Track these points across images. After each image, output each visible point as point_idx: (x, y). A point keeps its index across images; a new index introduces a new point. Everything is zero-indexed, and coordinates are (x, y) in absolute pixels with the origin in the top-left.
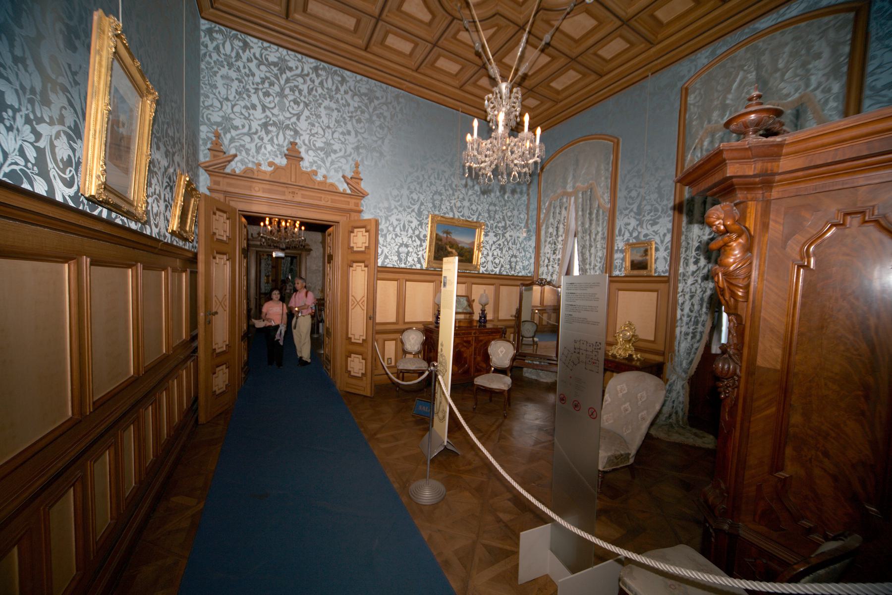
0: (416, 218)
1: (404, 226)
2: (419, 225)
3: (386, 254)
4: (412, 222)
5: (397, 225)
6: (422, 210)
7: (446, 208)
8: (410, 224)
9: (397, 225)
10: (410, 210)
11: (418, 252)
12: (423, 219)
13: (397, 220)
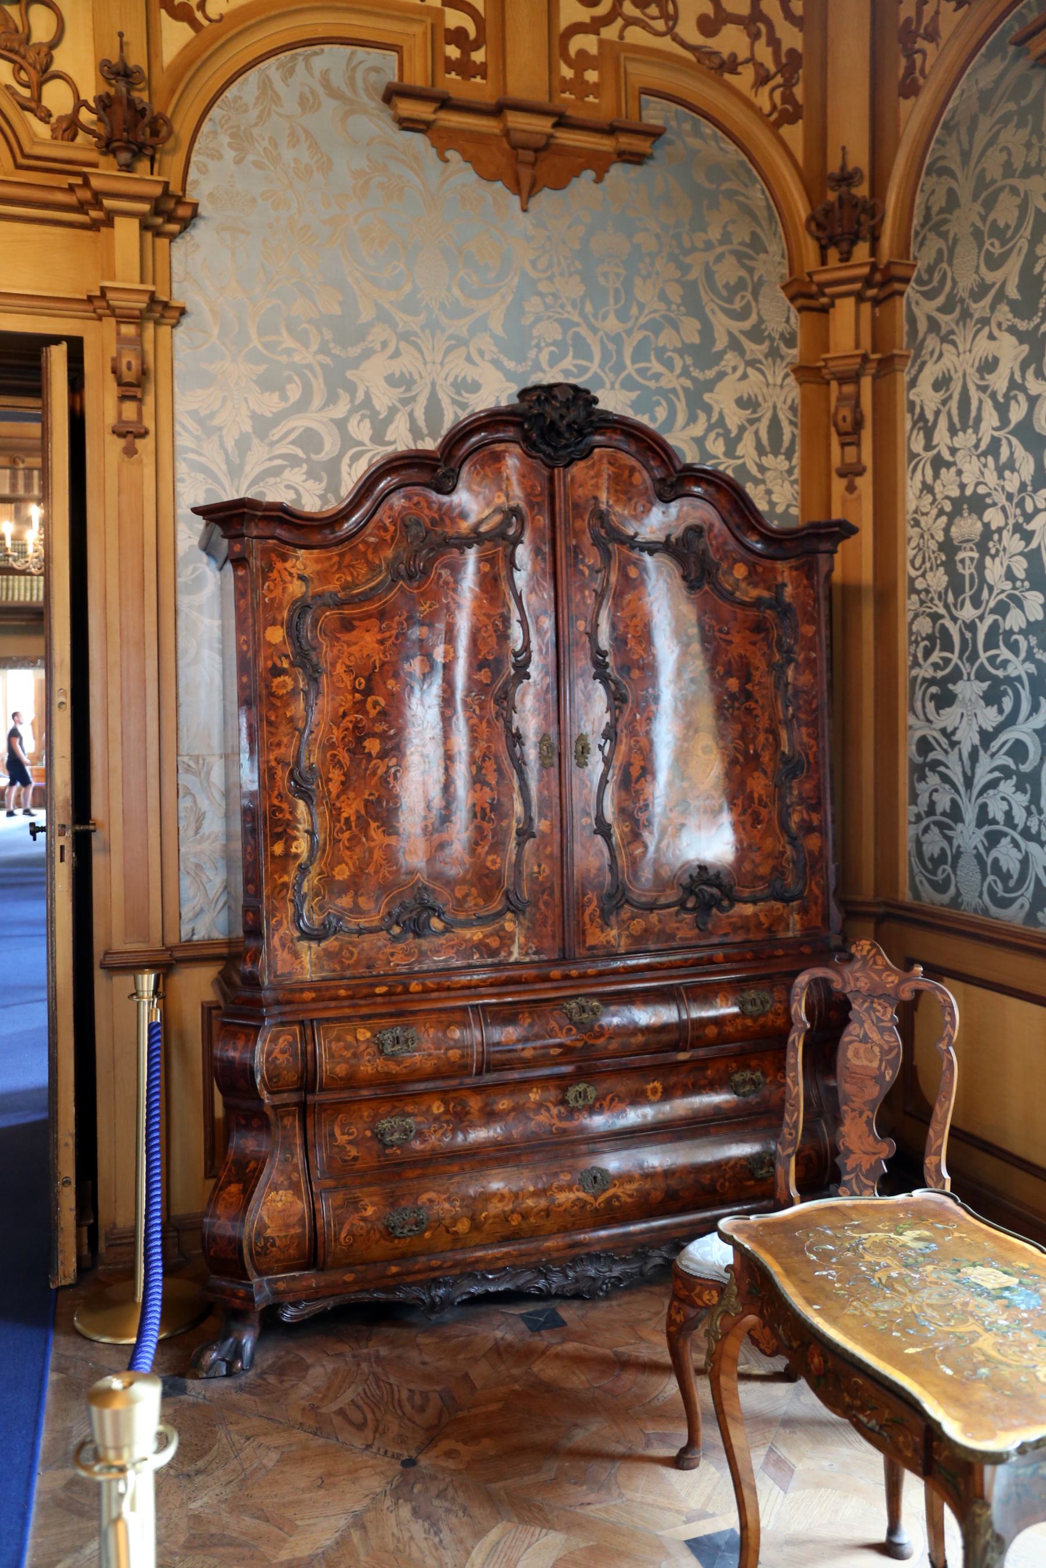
0: (496, 363)
9: (393, 411)
10: (461, 328)
13: (392, 381)
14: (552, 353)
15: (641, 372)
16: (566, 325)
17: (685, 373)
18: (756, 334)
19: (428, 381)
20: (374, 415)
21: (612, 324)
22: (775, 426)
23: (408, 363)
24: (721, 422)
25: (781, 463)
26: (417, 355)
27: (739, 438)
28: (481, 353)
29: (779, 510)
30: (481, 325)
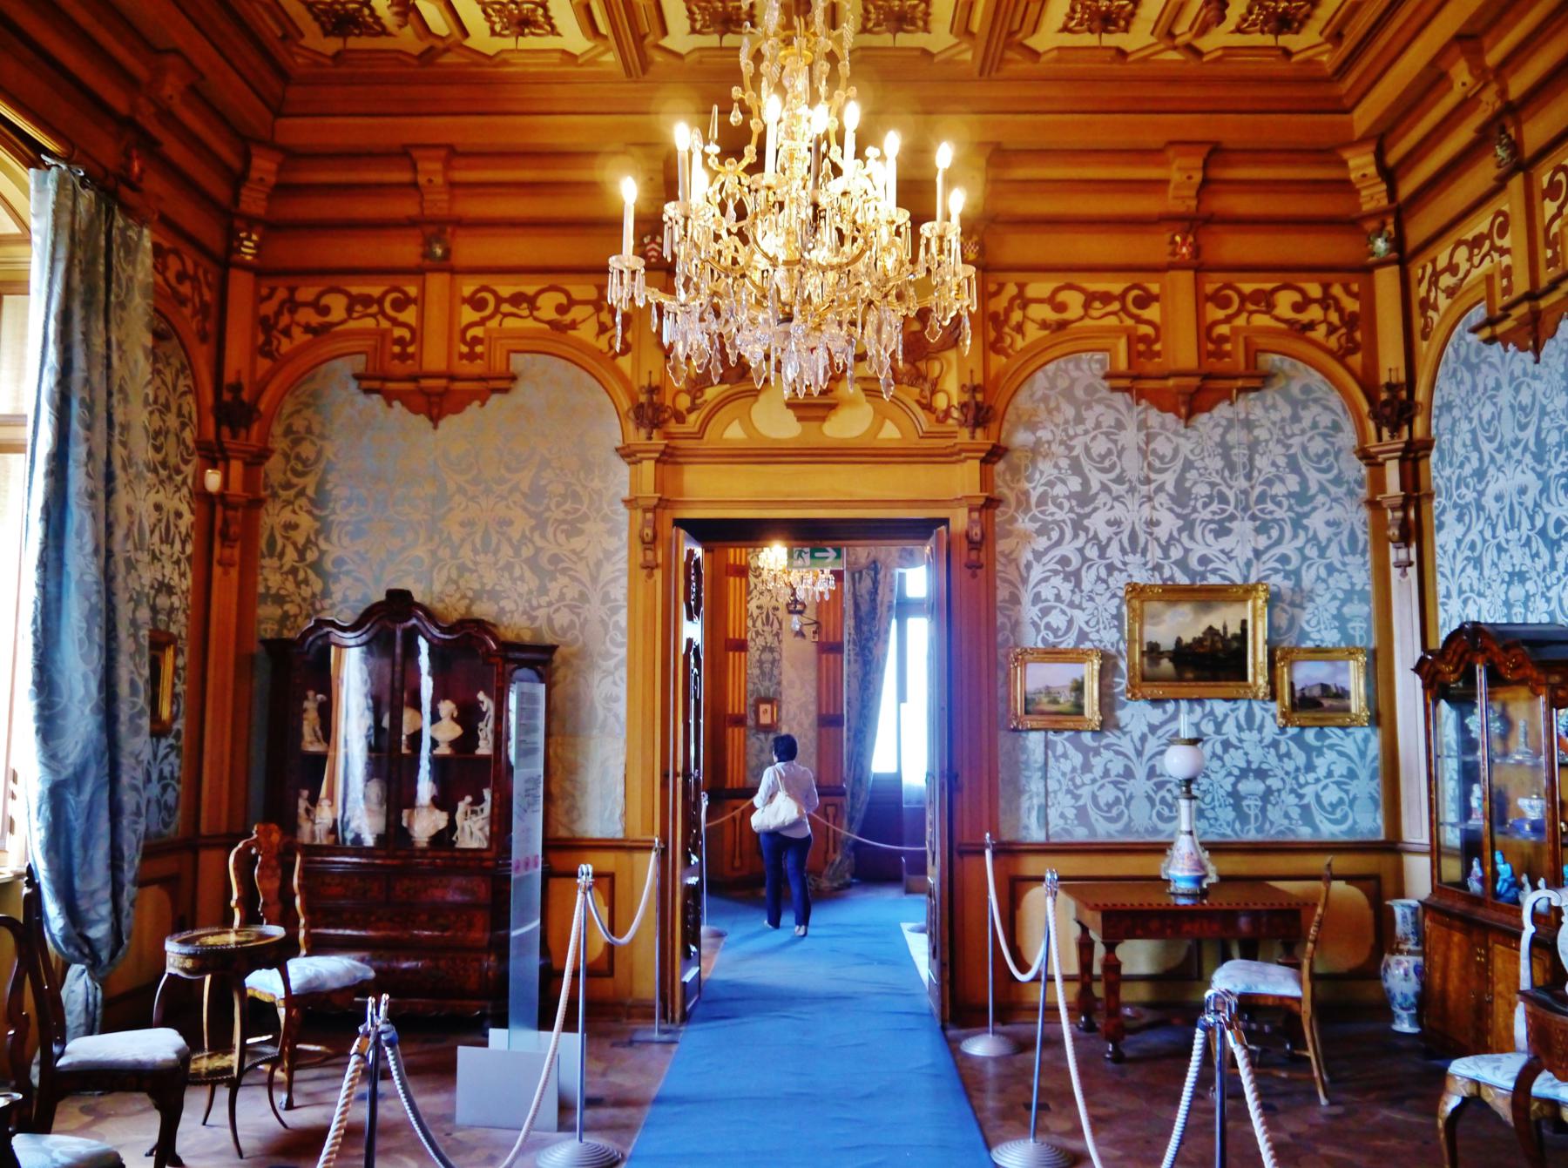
0: (1171, 510)
1: (1133, 537)
2: (1180, 530)
3: (1081, 629)
4: (1157, 523)
5: (1110, 539)
6: (1188, 484)
7: (1274, 464)
12: (1195, 510)
13: (1109, 523)
15: (1262, 511)
16: (1212, 485)
17: (1290, 509)
18: (1337, 481)
20: (1099, 544)
21: (1245, 484)
22: (1353, 537)
23: (1119, 511)
24: (1315, 537)
25: (1358, 560)
27: (1327, 546)
29: (1358, 588)
30: (1160, 488)
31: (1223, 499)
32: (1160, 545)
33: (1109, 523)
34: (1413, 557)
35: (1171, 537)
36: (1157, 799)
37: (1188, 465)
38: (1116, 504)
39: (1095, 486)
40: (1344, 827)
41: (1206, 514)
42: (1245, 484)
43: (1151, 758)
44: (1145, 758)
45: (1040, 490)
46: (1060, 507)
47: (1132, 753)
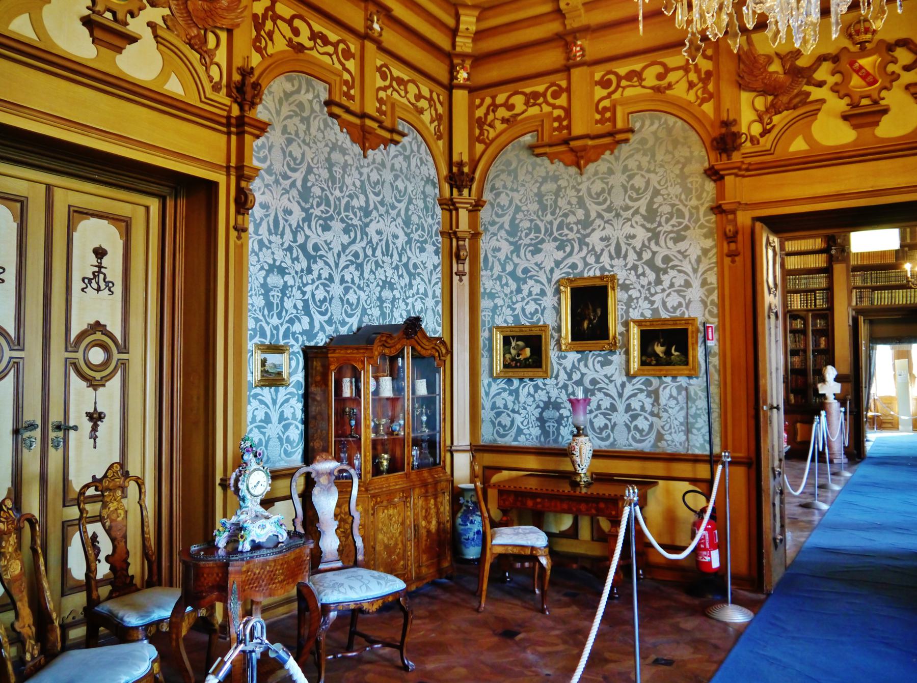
1: (618, 245)
2: (650, 240)
8: (631, 241)
9: (603, 250)
11: (652, 295)
14: (667, 218)
19: (616, 237)
23: (609, 231)
26: (611, 227)
28: (637, 223)
31: (681, 215)
32: (635, 251)
33: (602, 239)
34: (467, 270)
35: (643, 245)
36: (632, 426)
37: (656, 193)
38: (607, 225)
39: (593, 215)
40: (607, 443)
41: (527, 241)
42: (694, 202)
43: (628, 399)
44: (624, 399)
45: (559, 220)
46: (571, 230)
47: (615, 395)
